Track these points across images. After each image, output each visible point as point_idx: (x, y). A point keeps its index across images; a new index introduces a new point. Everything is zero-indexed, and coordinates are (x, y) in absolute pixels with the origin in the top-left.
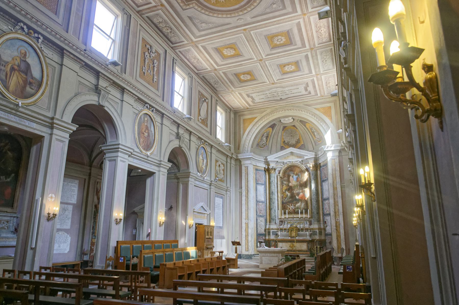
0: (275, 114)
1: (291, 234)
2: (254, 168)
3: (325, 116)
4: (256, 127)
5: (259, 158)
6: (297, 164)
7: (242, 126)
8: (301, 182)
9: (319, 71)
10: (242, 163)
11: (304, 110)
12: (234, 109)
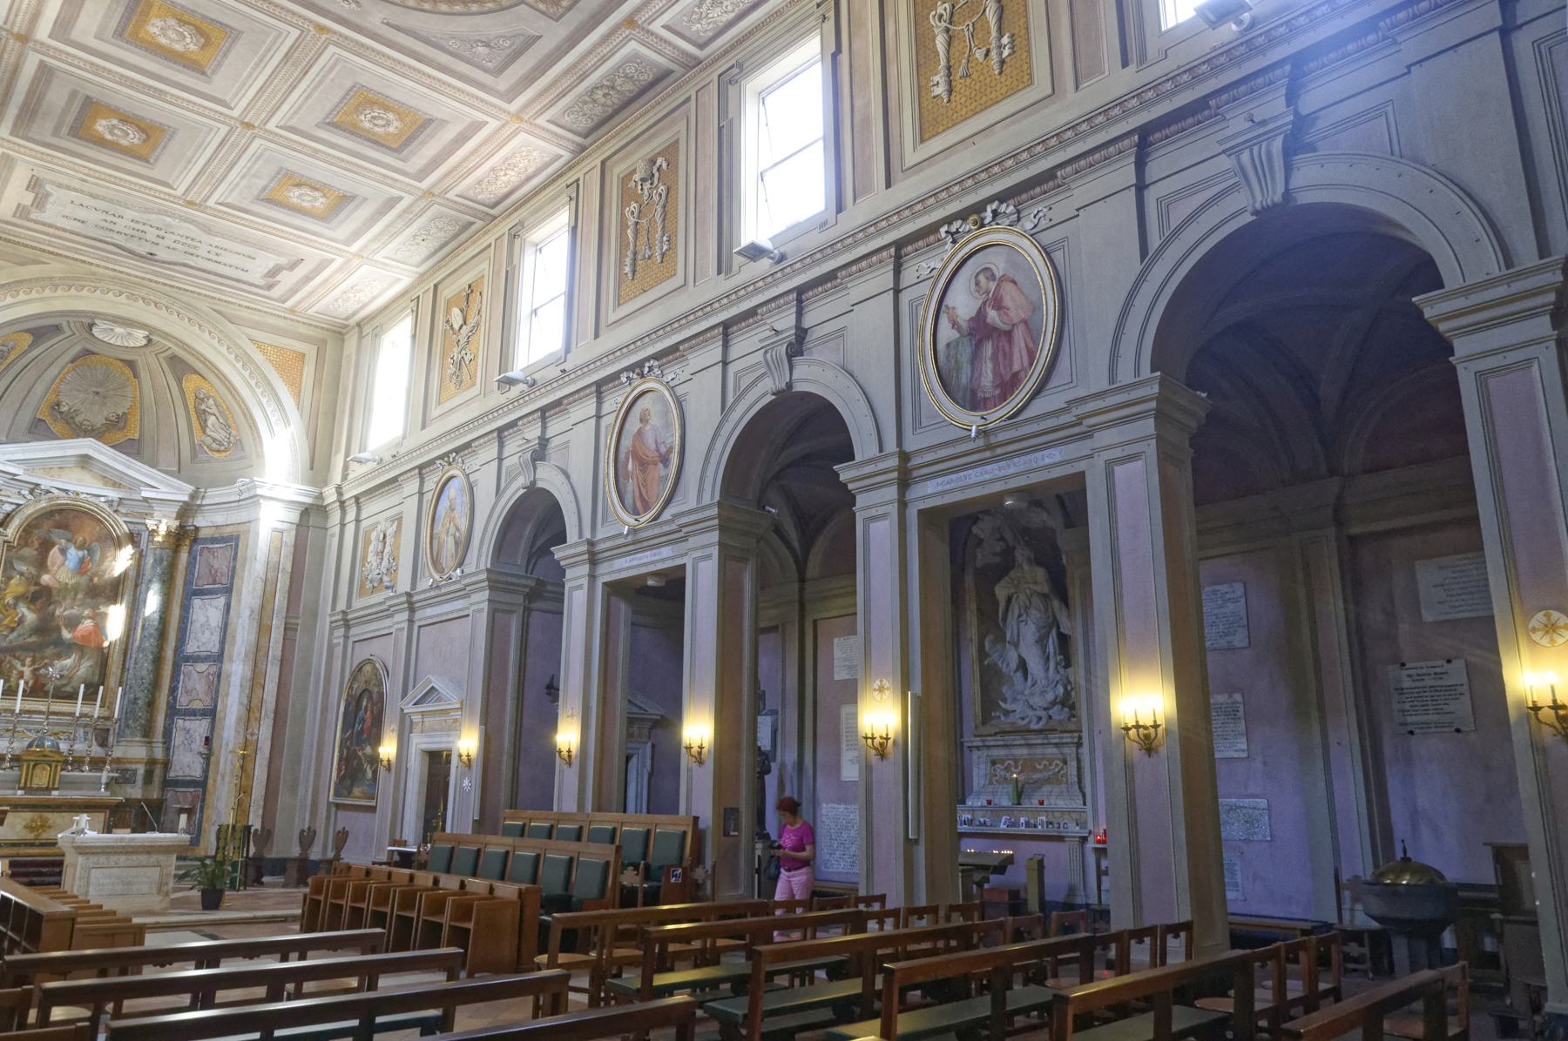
0: (85, 292)
1: (30, 775)
6: (97, 506)
8: (96, 579)
9: (375, 252)
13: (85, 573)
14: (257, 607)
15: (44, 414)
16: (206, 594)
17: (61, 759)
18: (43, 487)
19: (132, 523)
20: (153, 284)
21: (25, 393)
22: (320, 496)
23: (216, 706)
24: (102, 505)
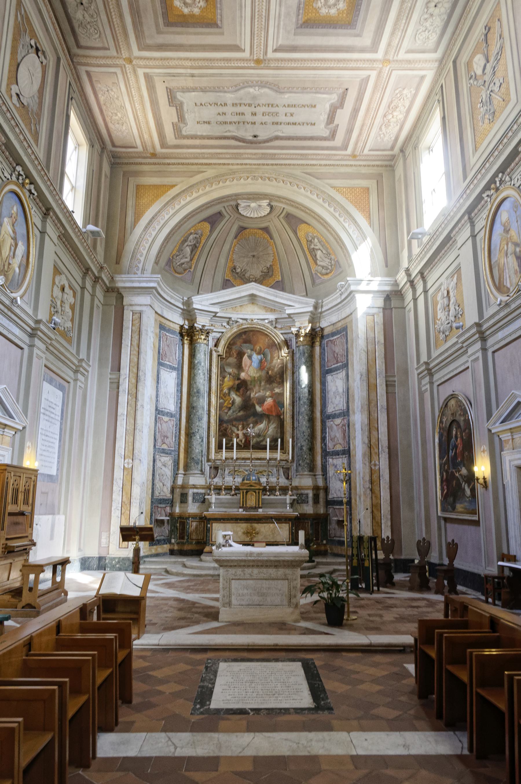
0: (228, 183)
1: (245, 500)
2: (156, 320)
3: (356, 209)
4: (172, 209)
5: (172, 297)
6: (264, 326)
7: (131, 202)
8: (270, 372)
10: (126, 301)
11: (304, 185)
12: (114, 145)
13: (264, 368)
14: (364, 371)
15: (229, 277)
16: (334, 371)
17: (261, 488)
18: (233, 319)
19: (285, 333)
20: (266, 167)
21: (215, 264)
22: (396, 284)
23: (349, 447)
24: (266, 325)
